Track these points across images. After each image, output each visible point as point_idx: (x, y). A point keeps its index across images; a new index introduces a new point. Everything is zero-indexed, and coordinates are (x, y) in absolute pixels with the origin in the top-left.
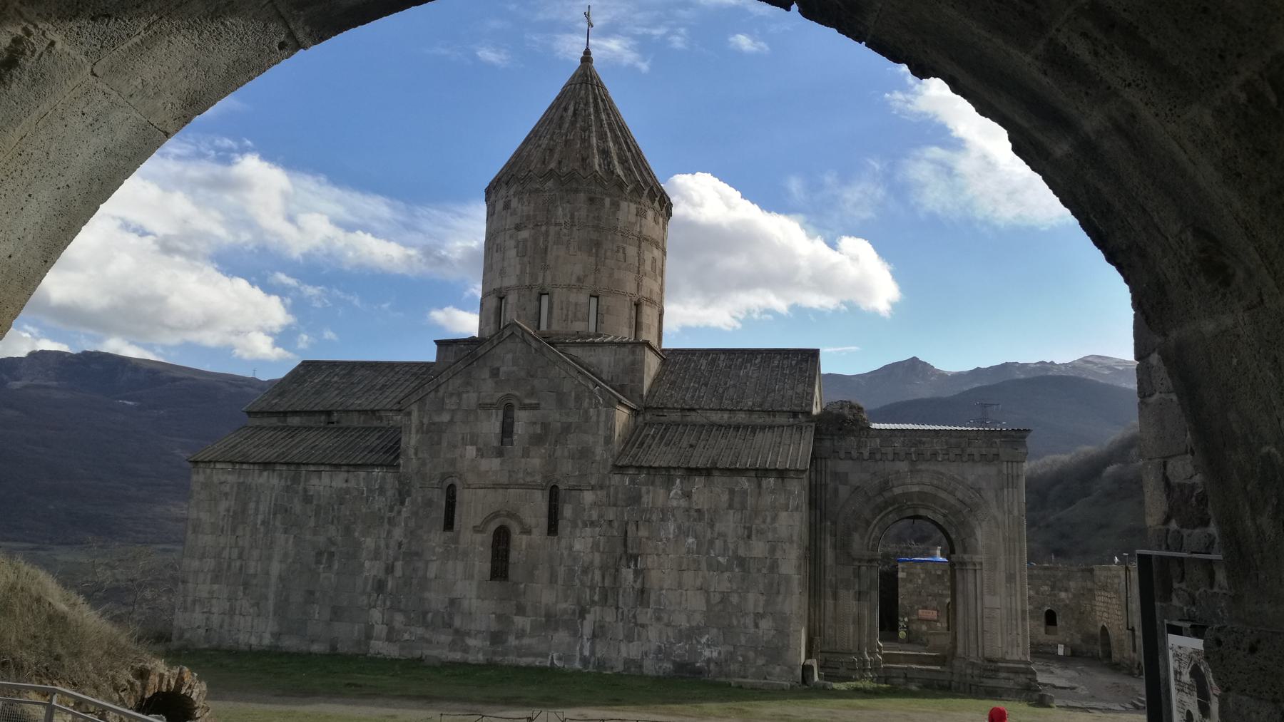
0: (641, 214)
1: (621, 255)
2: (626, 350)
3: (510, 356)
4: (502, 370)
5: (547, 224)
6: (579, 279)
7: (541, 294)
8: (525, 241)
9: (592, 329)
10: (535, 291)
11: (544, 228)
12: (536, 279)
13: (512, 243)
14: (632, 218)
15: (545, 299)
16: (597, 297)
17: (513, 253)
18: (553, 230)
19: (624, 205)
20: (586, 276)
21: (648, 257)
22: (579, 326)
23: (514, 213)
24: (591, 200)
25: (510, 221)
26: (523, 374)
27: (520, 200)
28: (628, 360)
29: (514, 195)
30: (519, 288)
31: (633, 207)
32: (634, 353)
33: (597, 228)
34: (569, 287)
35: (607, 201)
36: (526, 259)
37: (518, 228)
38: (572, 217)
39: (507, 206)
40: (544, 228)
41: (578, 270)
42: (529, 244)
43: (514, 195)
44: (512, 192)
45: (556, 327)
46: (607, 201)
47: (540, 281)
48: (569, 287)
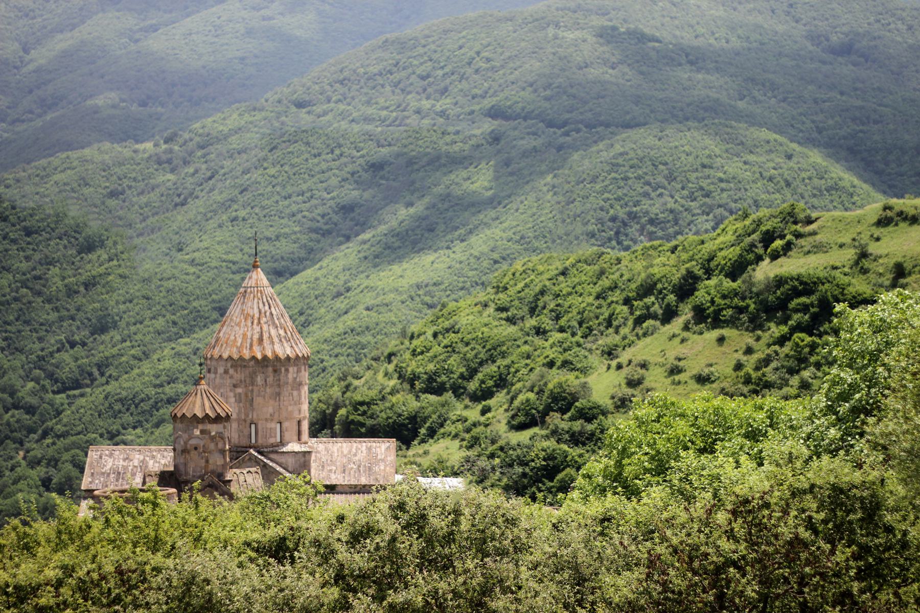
0: (299, 371)
5: (253, 385)
8: (240, 394)
9: (279, 440)
10: (248, 422)
13: (232, 394)
15: (253, 426)
17: (232, 400)
18: (256, 389)
19: (291, 369)
22: (272, 441)
23: (231, 377)
24: (275, 371)
25: (228, 381)
27: (236, 371)
28: (302, 460)
29: (232, 367)
31: (295, 368)
32: (304, 456)
33: (279, 386)
36: (241, 405)
37: (235, 386)
39: (226, 372)
41: (271, 410)
42: (243, 396)
44: (229, 365)
48: (266, 420)
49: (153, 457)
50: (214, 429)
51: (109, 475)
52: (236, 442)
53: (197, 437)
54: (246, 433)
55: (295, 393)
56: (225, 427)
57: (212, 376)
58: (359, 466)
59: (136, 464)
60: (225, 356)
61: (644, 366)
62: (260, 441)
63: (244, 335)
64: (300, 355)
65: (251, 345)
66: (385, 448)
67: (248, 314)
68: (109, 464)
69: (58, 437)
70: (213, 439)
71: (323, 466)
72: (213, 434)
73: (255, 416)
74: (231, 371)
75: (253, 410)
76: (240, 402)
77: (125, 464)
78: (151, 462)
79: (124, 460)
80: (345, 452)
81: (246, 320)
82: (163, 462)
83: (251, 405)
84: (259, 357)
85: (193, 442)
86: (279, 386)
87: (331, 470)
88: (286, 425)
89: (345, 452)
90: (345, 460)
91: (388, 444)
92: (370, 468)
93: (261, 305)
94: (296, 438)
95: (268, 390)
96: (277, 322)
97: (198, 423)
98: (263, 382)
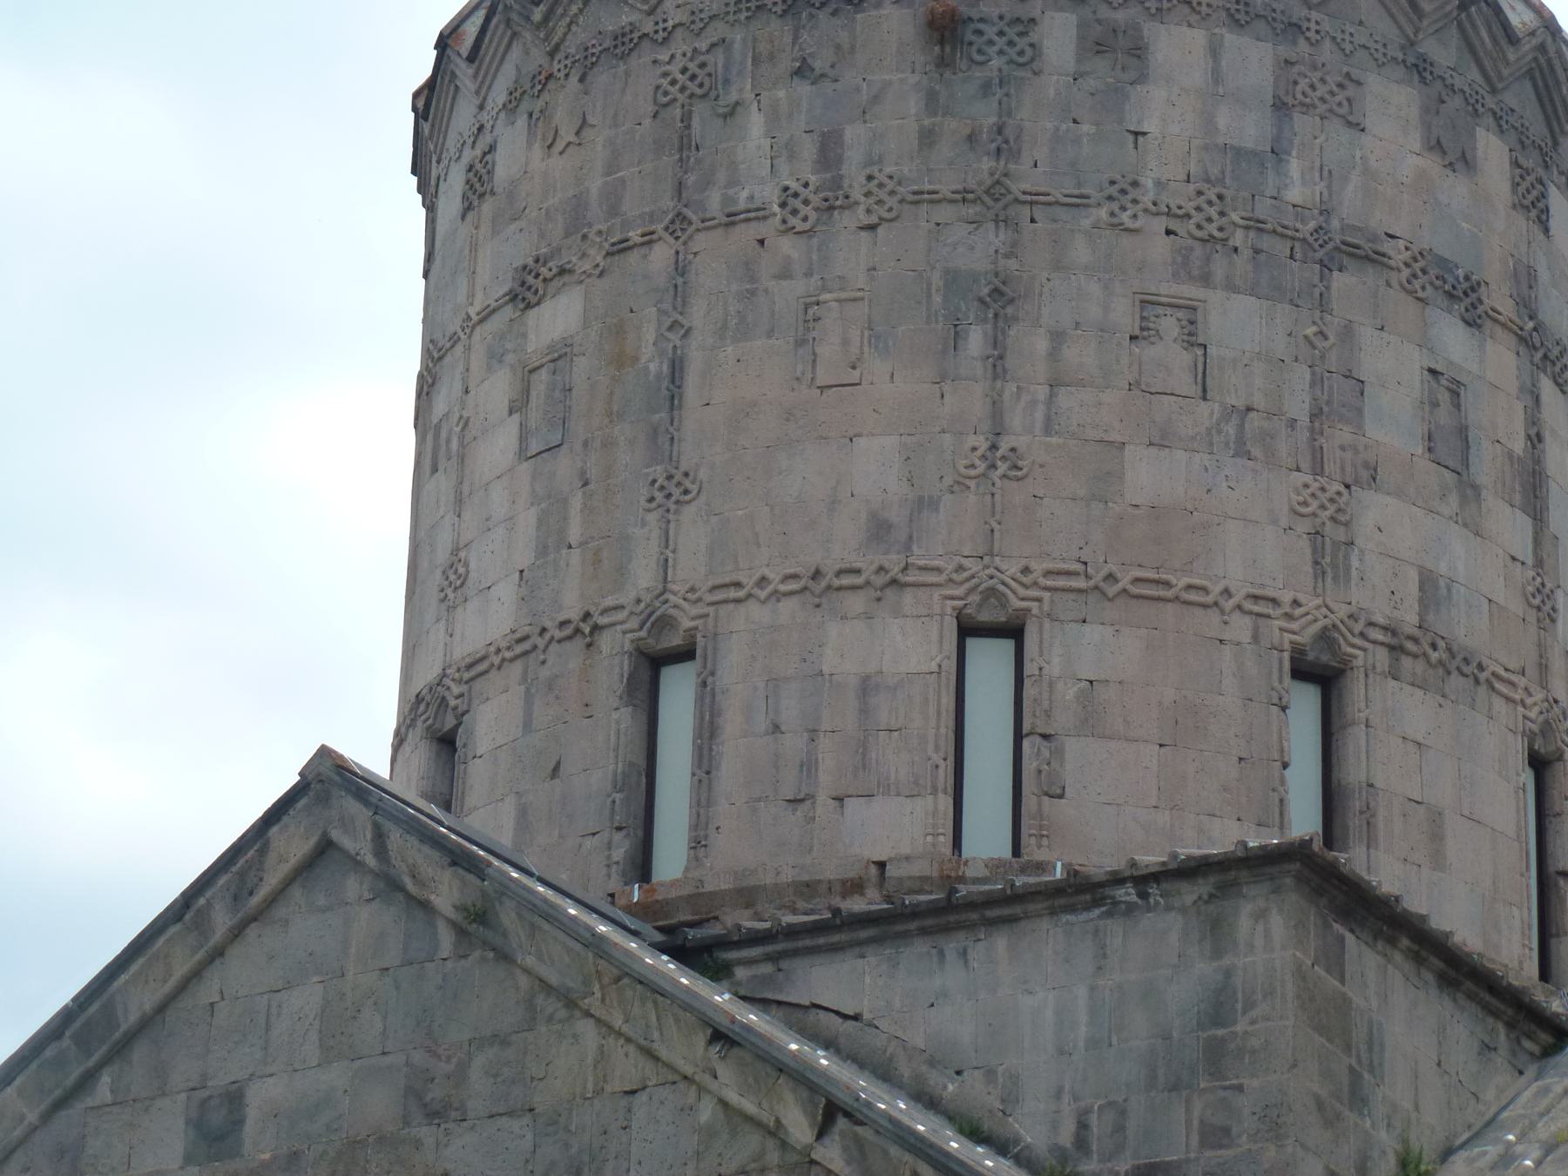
1: (1170, 359)
3: (306, 999)
4: (259, 1097)
6: (879, 529)
7: (652, 664)
8: (560, 355)
9: (987, 836)
10: (615, 646)
11: (661, 255)
12: (621, 572)
14: (1248, 128)
16: (1013, 632)
19: (1178, 47)
20: (923, 504)
21: (1392, 365)
26: (380, 1105)
30: (524, 647)
31: (1253, 60)
32: (1217, 935)
33: (994, 202)
34: (819, 587)
36: (564, 466)
37: (525, 293)
38: (829, 152)
39: (478, 185)
40: (661, 255)
41: (875, 469)
43: (510, 108)
44: (499, 96)
46: (1059, 36)
47: (643, 577)
48: (819, 587)
55: (1241, 323)
73: (691, 567)
74: (514, 153)
75: (673, 491)
83: (662, 441)
88: (1074, 650)
98: (804, 170)
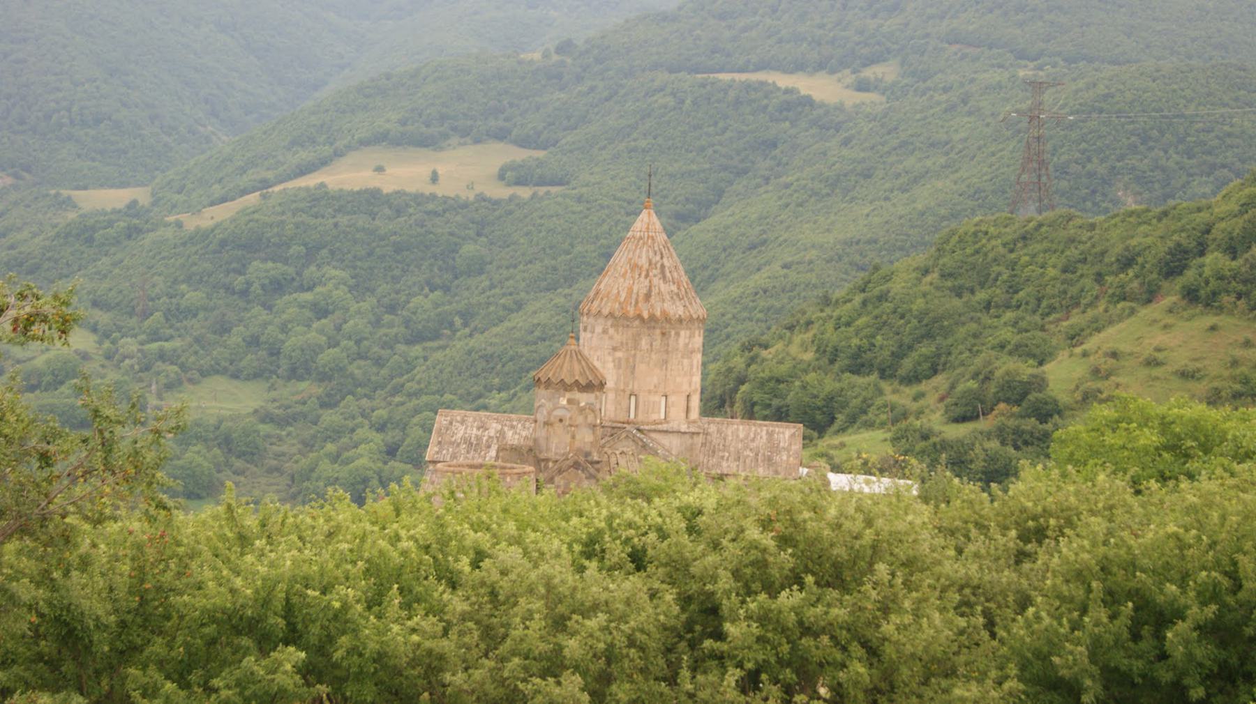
2: (687, 436)
8: (620, 359)
9: (662, 416)
13: (610, 359)
15: (633, 398)
17: (611, 365)
18: (639, 355)
19: (682, 333)
22: (654, 417)
23: (611, 338)
24: (663, 334)
27: (617, 331)
33: (667, 352)
34: (650, 392)
35: (673, 333)
37: (615, 349)
39: (605, 331)
41: (655, 380)
44: (609, 323)
45: (640, 418)
46: (673, 333)
48: (650, 392)
49: (512, 427)
50: (584, 399)
51: (458, 445)
52: (612, 416)
53: (564, 407)
54: (624, 404)
55: (686, 361)
56: (596, 398)
57: (589, 335)
58: (757, 455)
59: (492, 434)
60: (606, 311)
61: (1114, 355)
62: (640, 418)
63: (630, 290)
64: (695, 316)
65: (637, 303)
66: (788, 434)
67: (636, 265)
68: (460, 432)
69: (410, 395)
70: (582, 410)
71: (714, 452)
72: (582, 404)
73: (636, 387)
74: (611, 331)
76: (619, 368)
77: (479, 433)
78: (510, 434)
79: (478, 429)
80: (742, 435)
81: (632, 270)
82: (524, 434)
83: (633, 373)
84: (646, 315)
85: (559, 413)
86: (667, 352)
87: (722, 457)
88: (672, 399)
89: (742, 435)
90: (740, 446)
91: (793, 431)
92: (770, 459)
93: (651, 254)
94: (683, 415)
95: (654, 356)
96: (668, 274)
97: (566, 390)
